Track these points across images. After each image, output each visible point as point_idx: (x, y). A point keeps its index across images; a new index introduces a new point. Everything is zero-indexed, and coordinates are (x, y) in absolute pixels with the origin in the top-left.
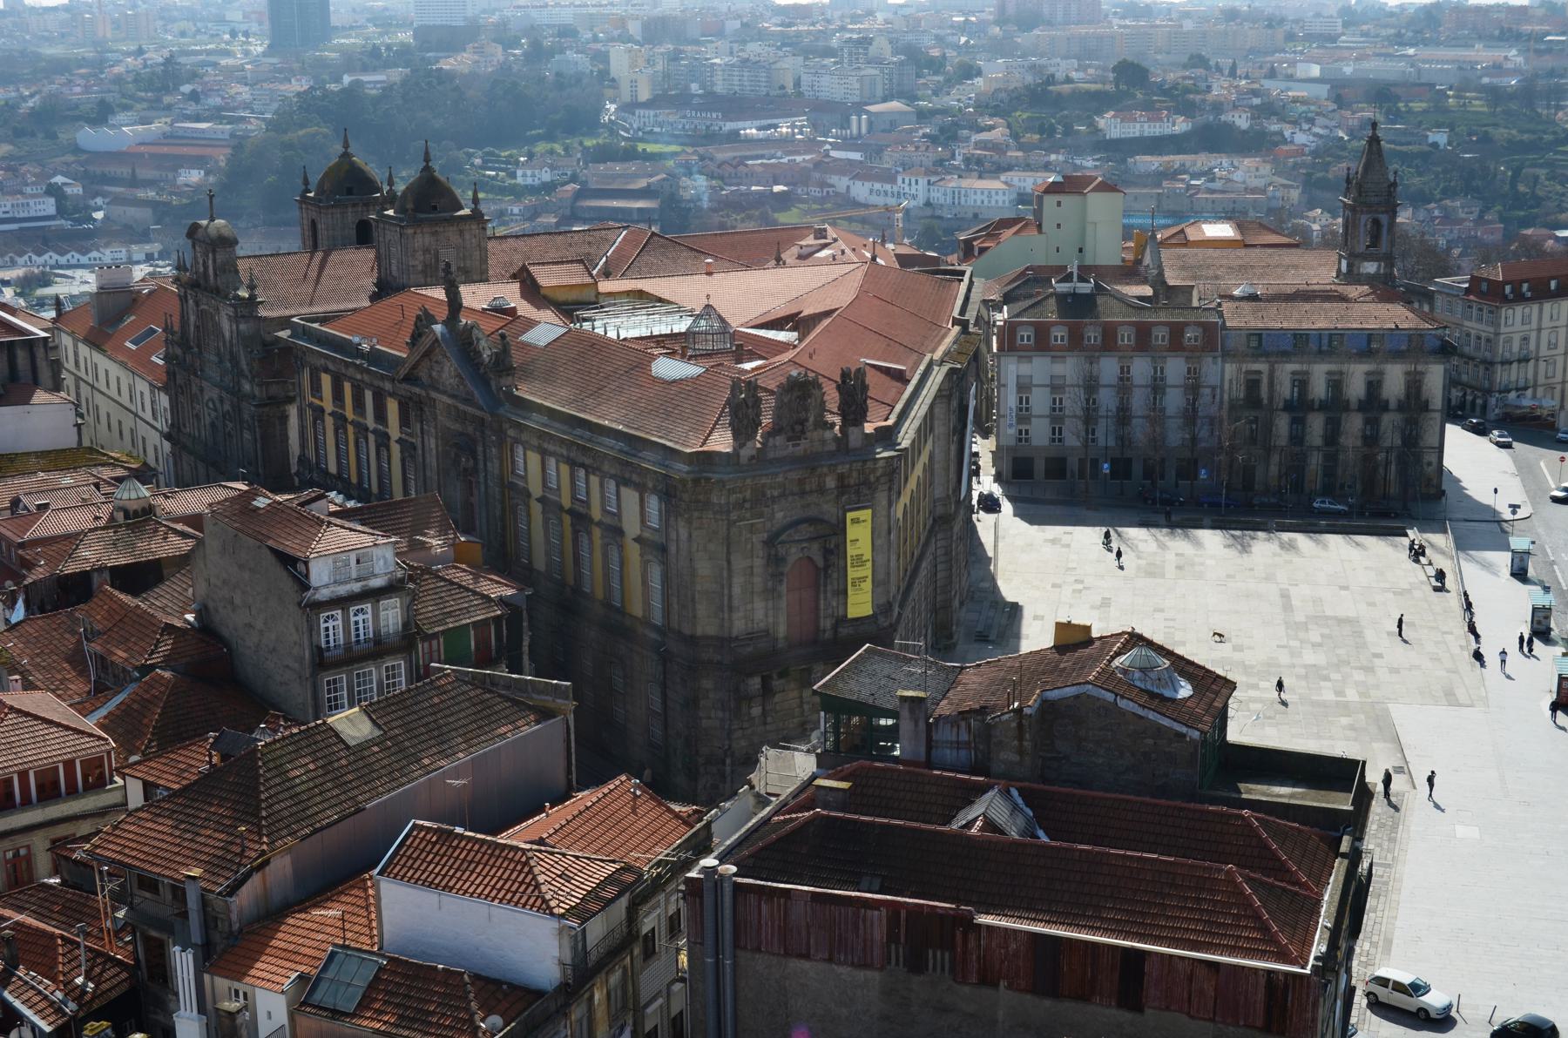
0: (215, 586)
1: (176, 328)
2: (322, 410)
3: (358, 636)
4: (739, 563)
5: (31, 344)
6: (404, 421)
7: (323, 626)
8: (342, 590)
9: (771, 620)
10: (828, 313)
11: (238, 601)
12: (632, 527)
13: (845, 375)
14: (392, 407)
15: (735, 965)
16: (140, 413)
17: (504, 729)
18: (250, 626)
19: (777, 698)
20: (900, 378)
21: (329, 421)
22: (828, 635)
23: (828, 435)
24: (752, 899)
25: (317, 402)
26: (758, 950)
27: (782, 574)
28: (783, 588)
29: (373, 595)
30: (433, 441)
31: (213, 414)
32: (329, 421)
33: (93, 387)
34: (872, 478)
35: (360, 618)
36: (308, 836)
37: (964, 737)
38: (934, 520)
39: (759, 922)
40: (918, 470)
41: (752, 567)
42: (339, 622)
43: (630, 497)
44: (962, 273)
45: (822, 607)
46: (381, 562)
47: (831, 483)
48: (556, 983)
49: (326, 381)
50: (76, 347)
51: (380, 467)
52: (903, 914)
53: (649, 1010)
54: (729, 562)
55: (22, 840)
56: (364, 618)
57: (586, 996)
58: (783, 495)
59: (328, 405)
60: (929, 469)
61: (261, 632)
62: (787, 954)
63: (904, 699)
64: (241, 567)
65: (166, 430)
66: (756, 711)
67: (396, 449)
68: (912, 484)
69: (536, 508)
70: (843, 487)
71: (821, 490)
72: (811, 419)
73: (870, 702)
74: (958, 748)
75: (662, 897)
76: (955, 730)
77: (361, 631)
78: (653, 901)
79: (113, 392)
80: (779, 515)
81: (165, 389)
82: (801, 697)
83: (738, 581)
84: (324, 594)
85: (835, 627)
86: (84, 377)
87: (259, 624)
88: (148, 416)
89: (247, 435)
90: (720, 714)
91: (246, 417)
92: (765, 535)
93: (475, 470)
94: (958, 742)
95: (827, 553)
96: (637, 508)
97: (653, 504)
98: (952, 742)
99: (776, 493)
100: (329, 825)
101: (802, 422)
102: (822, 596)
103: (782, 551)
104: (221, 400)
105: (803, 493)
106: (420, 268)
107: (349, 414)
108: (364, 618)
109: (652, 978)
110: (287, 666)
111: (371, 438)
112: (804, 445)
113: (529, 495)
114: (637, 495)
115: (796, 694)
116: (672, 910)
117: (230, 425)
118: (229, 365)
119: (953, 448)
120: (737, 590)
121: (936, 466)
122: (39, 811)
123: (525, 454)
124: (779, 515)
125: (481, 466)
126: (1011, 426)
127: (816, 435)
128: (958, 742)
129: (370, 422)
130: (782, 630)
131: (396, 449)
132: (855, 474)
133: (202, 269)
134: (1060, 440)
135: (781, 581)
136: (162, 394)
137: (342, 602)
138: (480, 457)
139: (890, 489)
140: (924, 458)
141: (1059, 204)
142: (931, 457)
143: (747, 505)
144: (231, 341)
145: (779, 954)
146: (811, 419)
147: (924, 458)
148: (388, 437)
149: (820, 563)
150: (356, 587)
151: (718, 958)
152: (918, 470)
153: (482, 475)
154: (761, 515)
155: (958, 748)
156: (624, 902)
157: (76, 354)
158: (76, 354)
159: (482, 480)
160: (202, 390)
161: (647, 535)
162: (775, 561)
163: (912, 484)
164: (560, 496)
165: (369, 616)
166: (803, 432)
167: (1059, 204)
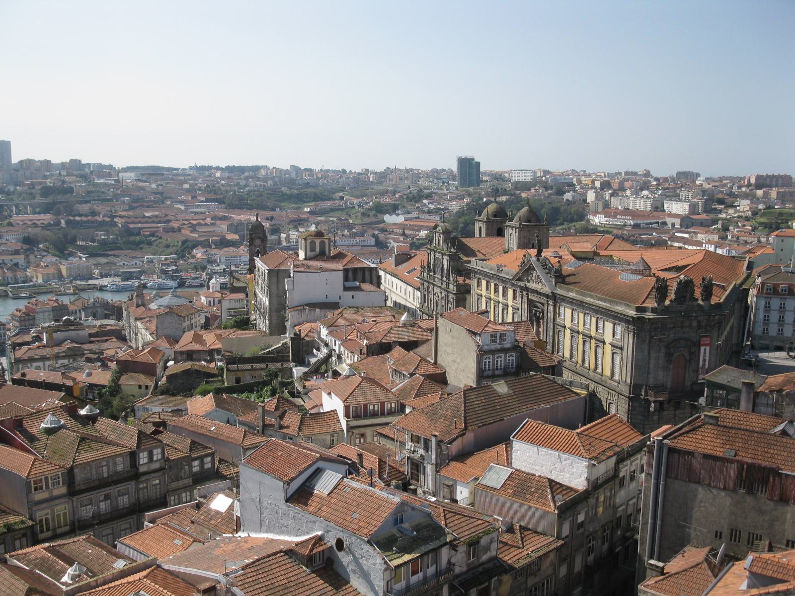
0: (442, 346)
1: (426, 265)
2: (481, 296)
3: (497, 367)
4: (653, 355)
5: (371, 270)
6: (514, 298)
7: (484, 361)
8: (493, 347)
9: (665, 380)
10: (690, 265)
11: (450, 351)
12: (608, 338)
13: (704, 279)
14: (510, 293)
15: (665, 486)
16: (408, 299)
17: (560, 398)
18: (455, 361)
19: (665, 413)
20: (724, 288)
21: (484, 299)
22: (689, 388)
23: (695, 303)
24: (676, 455)
25: (479, 292)
26: (677, 478)
27: (671, 360)
28: (671, 367)
29: (505, 351)
30: (526, 305)
31: (437, 298)
32: (484, 299)
33: (390, 290)
34: (712, 323)
35: (499, 359)
36: (479, 427)
37: (770, 402)
38: (732, 352)
39: (678, 466)
40: (728, 328)
41: (659, 356)
42: (491, 360)
43: (609, 326)
44: (746, 258)
45: (687, 375)
46: (509, 338)
47: (695, 324)
48: (585, 488)
49: (484, 283)
50: (385, 275)
51: (503, 317)
52: (745, 466)
53: (620, 509)
54: (649, 353)
55: (362, 430)
56: (501, 359)
57: (596, 496)
58: (674, 327)
59: (484, 293)
60: (732, 329)
61: (459, 363)
62: (689, 481)
63: (744, 383)
64: (453, 337)
65: (418, 306)
66: (656, 418)
67: (510, 309)
68: (725, 333)
69: (568, 332)
70: (699, 326)
71: (690, 326)
72: (688, 296)
73: (728, 384)
74: (767, 407)
75: (628, 462)
76: (766, 398)
77: (499, 365)
78: (625, 463)
79: (398, 292)
80: (672, 336)
81: (418, 289)
82: (675, 414)
83: (652, 362)
84: (486, 348)
85: (692, 386)
86: (388, 287)
87: (458, 360)
88: (411, 300)
89: (450, 306)
90: (640, 417)
91: (450, 298)
92: (666, 343)
93: (543, 316)
94: (767, 404)
95: (691, 353)
96: (611, 331)
97: (619, 329)
98: (765, 404)
99: (671, 326)
100: (489, 424)
101: (684, 297)
102: (687, 372)
103: (672, 350)
104: (441, 293)
105: (682, 327)
106: (522, 244)
107: (492, 296)
108: (501, 359)
109: (621, 496)
110: (468, 377)
111: (501, 305)
112: (684, 307)
113: (565, 327)
114: (611, 325)
115: (673, 412)
116: (633, 469)
117: (443, 302)
118: (445, 279)
119: (742, 323)
120: (652, 366)
121: (735, 330)
122: (370, 420)
123: (565, 310)
124: (672, 336)
125: (545, 315)
126: (760, 326)
127: (690, 303)
128: (767, 404)
129: (501, 299)
130: (669, 385)
131: (510, 309)
132: (705, 321)
133: (437, 242)
134: (781, 334)
135: (671, 363)
136: (418, 291)
137: (493, 352)
138: (546, 311)
139: (719, 329)
140: (730, 324)
141: (783, 241)
142: (733, 324)
143: (659, 330)
144: (447, 270)
145: (685, 481)
146: (688, 296)
147: (730, 324)
148: (508, 305)
149: (688, 358)
150: (499, 347)
151: (658, 481)
152: (728, 328)
153: (545, 318)
154: (664, 335)
155: (767, 407)
156: (614, 459)
157: (385, 278)
158: (385, 278)
159: (545, 320)
160: (433, 290)
161: (614, 341)
162: (669, 355)
163: (725, 333)
164: (578, 326)
165: (503, 359)
166: (685, 301)
167: (783, 241)
